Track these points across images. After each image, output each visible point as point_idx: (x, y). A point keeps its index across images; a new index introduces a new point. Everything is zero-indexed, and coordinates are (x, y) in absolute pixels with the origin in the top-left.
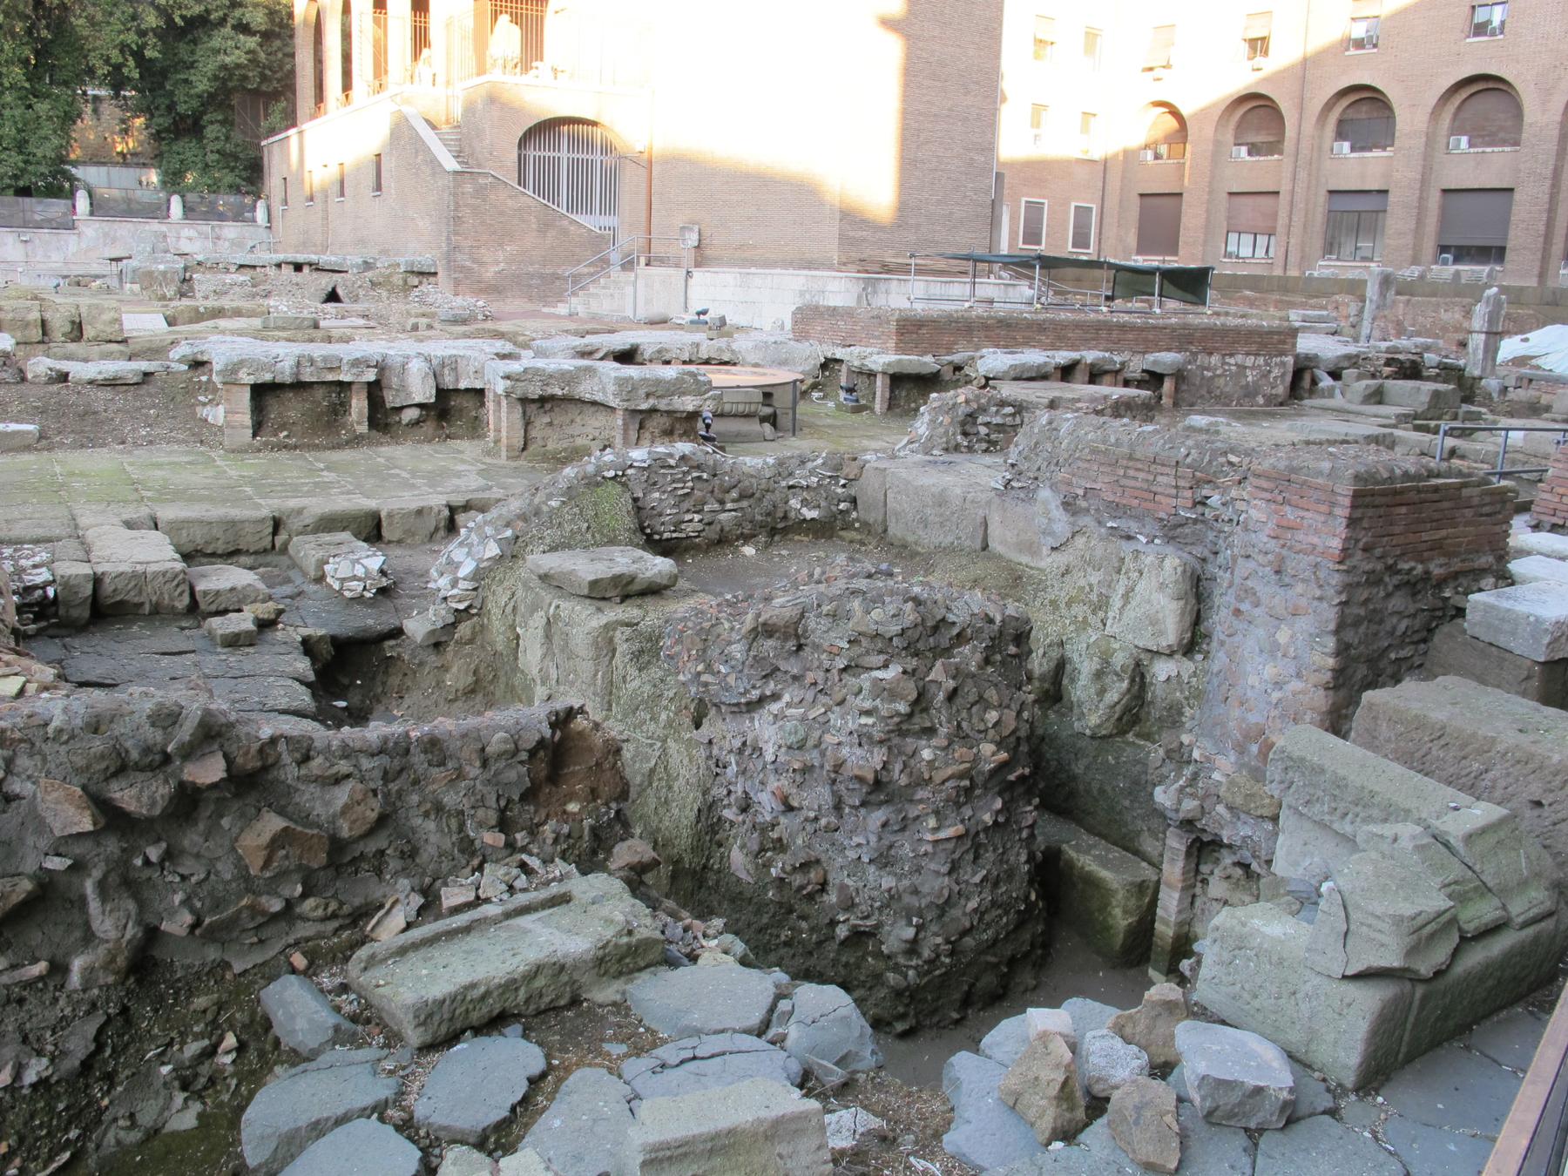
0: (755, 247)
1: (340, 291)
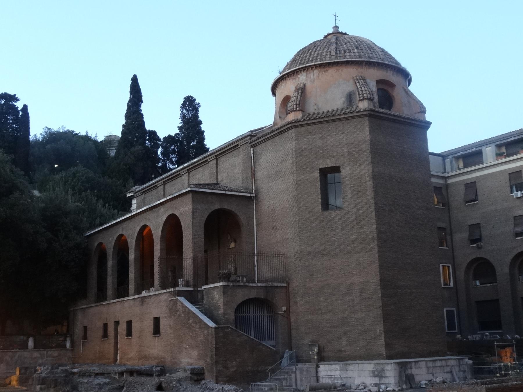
0: (345, 351)
1: (163, 385)
